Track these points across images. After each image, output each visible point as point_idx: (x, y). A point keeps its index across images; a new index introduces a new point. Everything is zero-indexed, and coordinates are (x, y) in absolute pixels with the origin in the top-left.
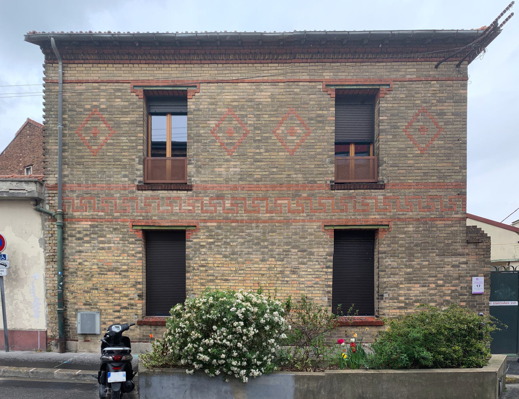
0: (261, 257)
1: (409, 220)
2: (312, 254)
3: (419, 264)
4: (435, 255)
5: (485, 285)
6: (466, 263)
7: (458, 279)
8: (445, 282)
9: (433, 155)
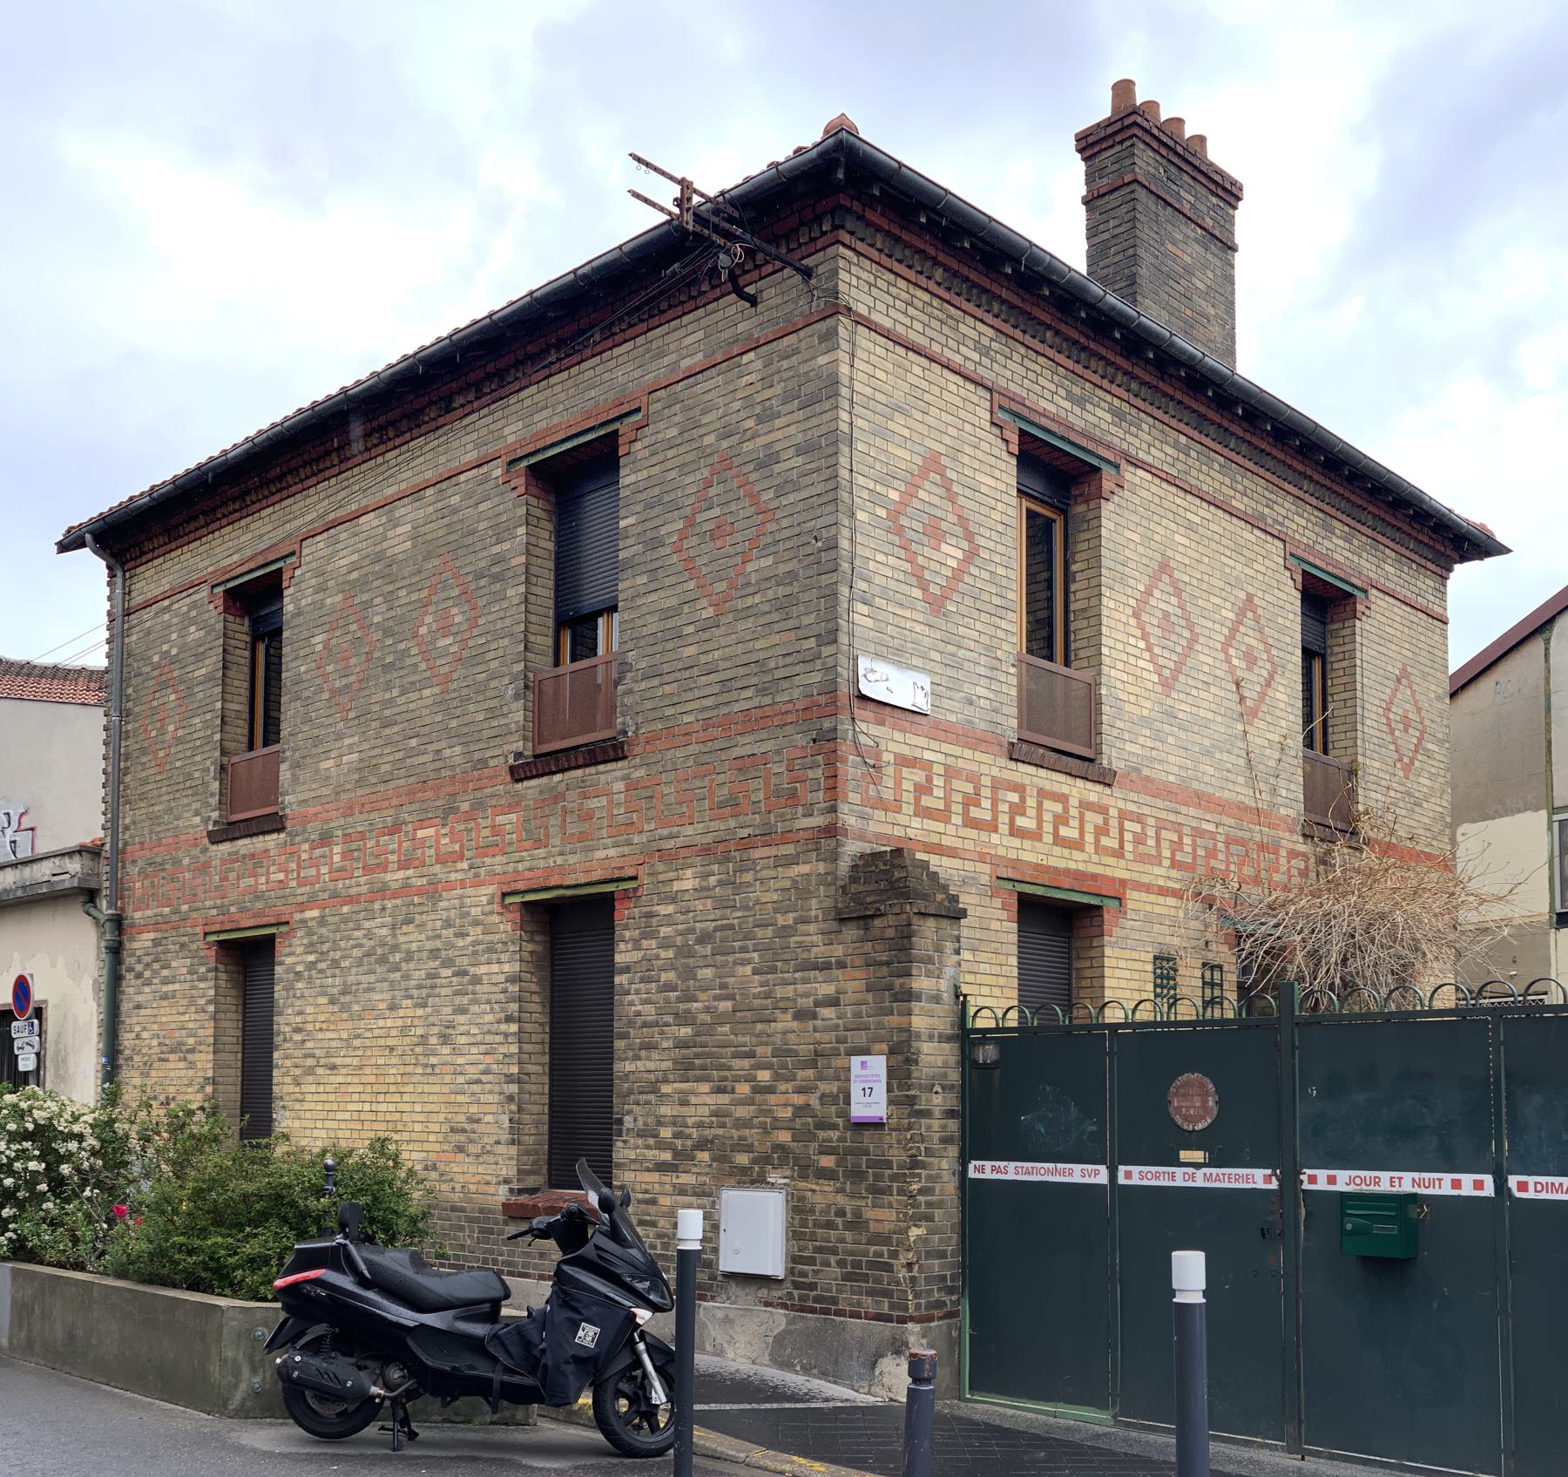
0: (387, 996)
1: (683, 853)
2: (477, 980)
3: (707, 1010)
4: (748, 969)
5: (889, 1090)
6: (833, 1002)
7: (812, 1064)
8: (777, 1077)
9: (747, 614)
